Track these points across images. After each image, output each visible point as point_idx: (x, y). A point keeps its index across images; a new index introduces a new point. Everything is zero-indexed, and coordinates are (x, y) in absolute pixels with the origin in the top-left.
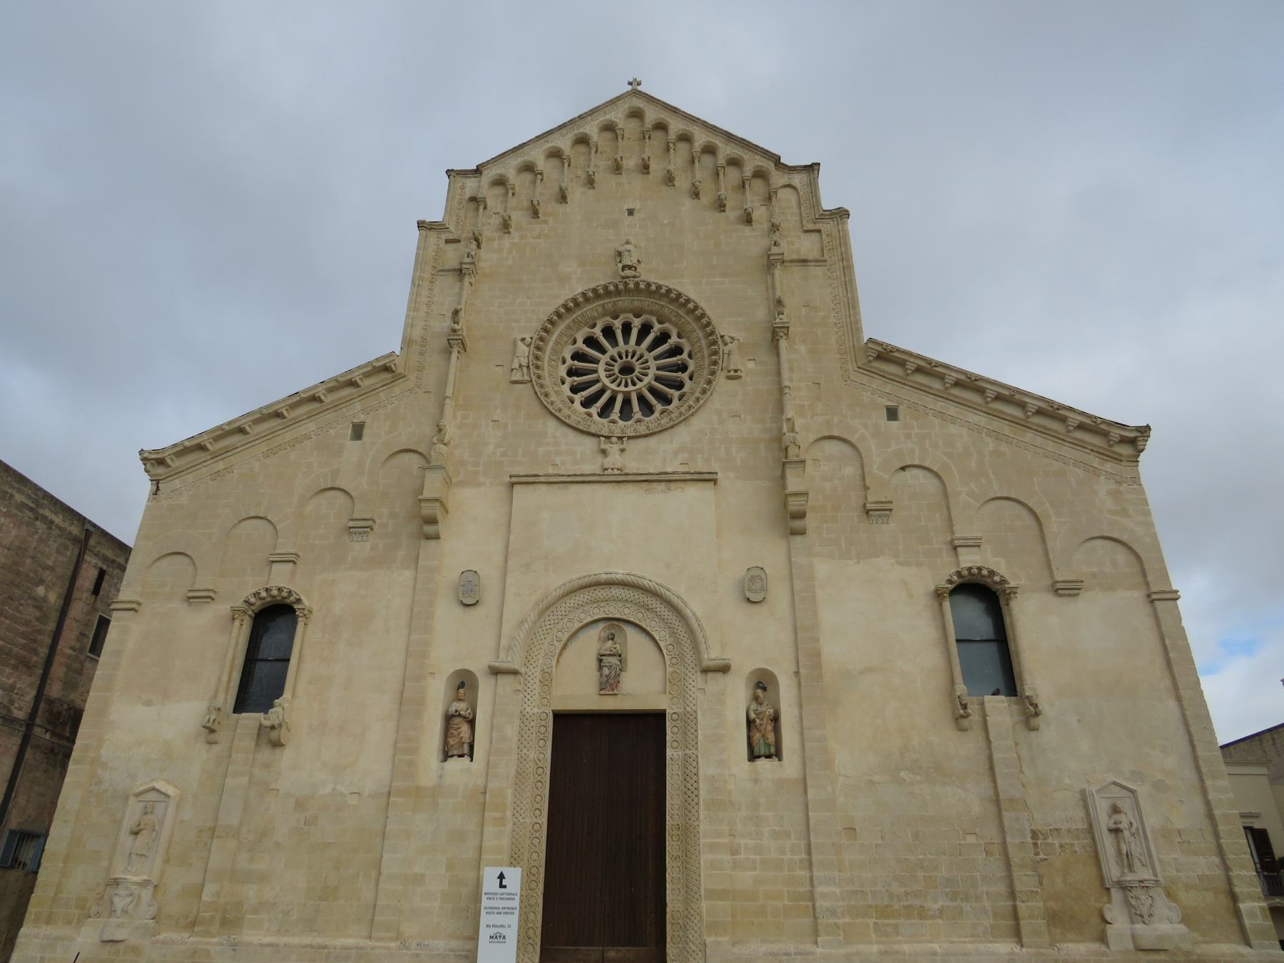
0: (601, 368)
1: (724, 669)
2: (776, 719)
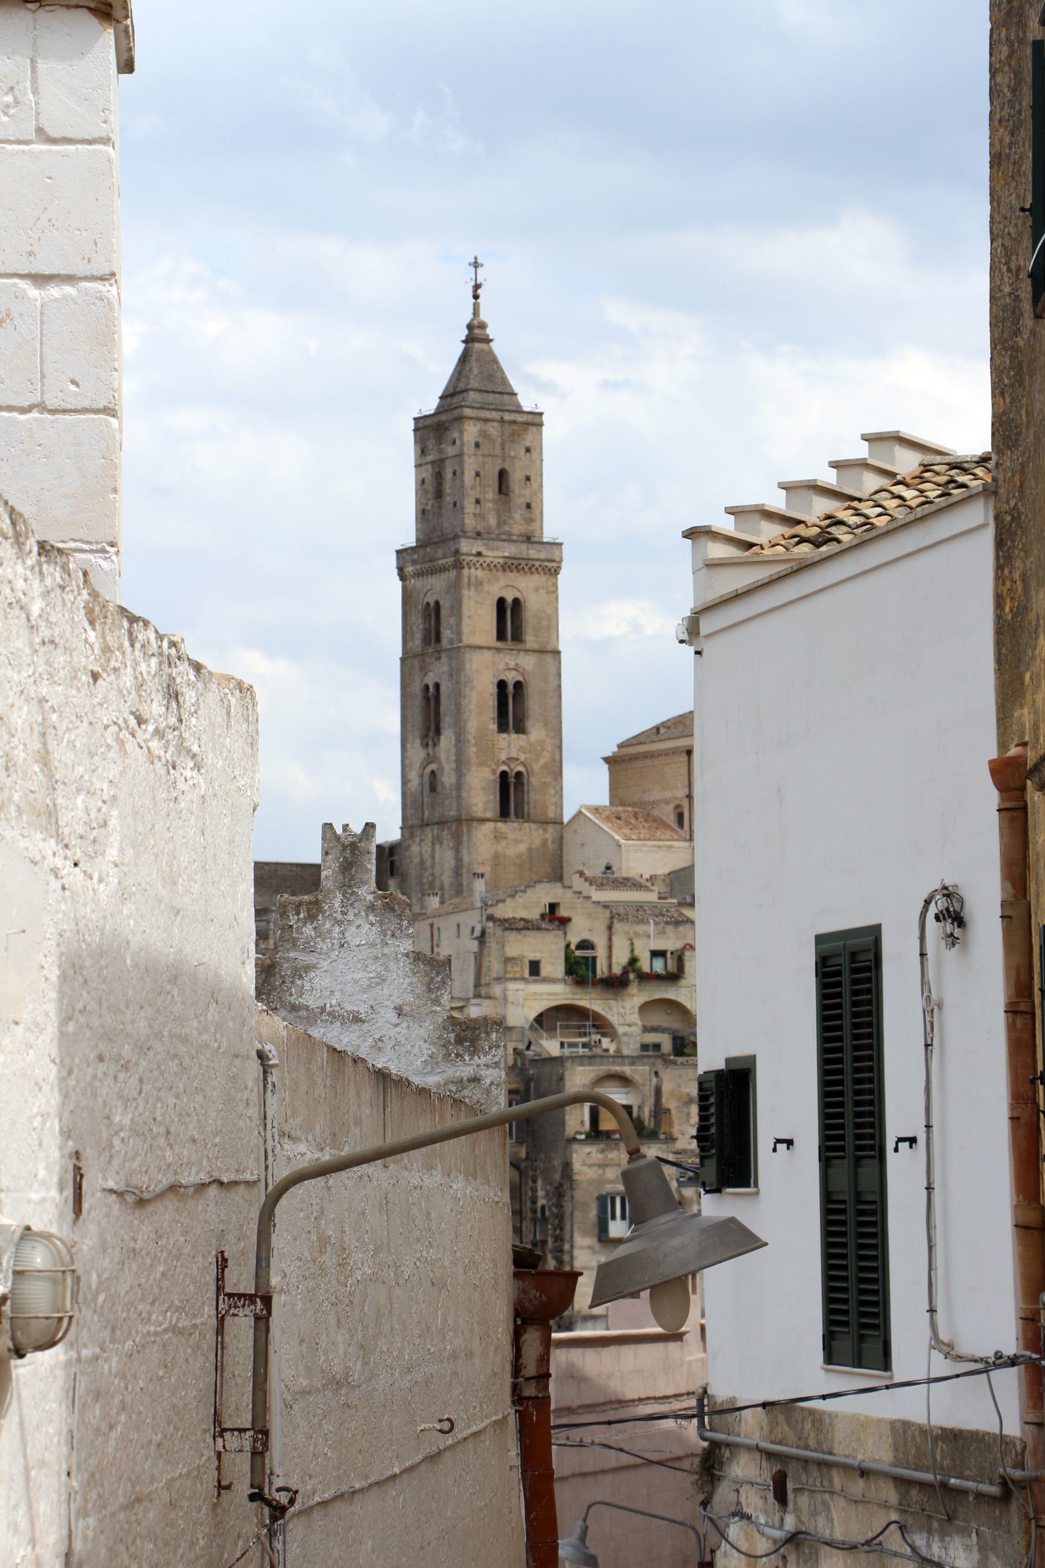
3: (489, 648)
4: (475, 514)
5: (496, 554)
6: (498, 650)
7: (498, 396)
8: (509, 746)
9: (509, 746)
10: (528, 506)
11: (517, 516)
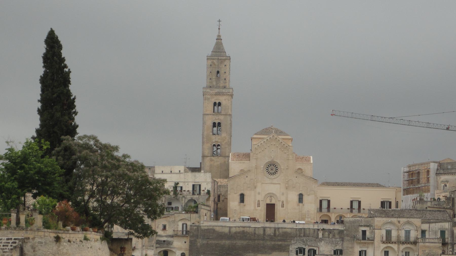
0: (269, 170)
1: (280, 201)
2: (284, 204)
3: (211, 114)
4: (209, 82)
5: (213, 91)
6: (213, 115)
7: (220, 53)
8: (215, 138)
9: (215, 138)
10: (225, 79)
11: (222, 82)
